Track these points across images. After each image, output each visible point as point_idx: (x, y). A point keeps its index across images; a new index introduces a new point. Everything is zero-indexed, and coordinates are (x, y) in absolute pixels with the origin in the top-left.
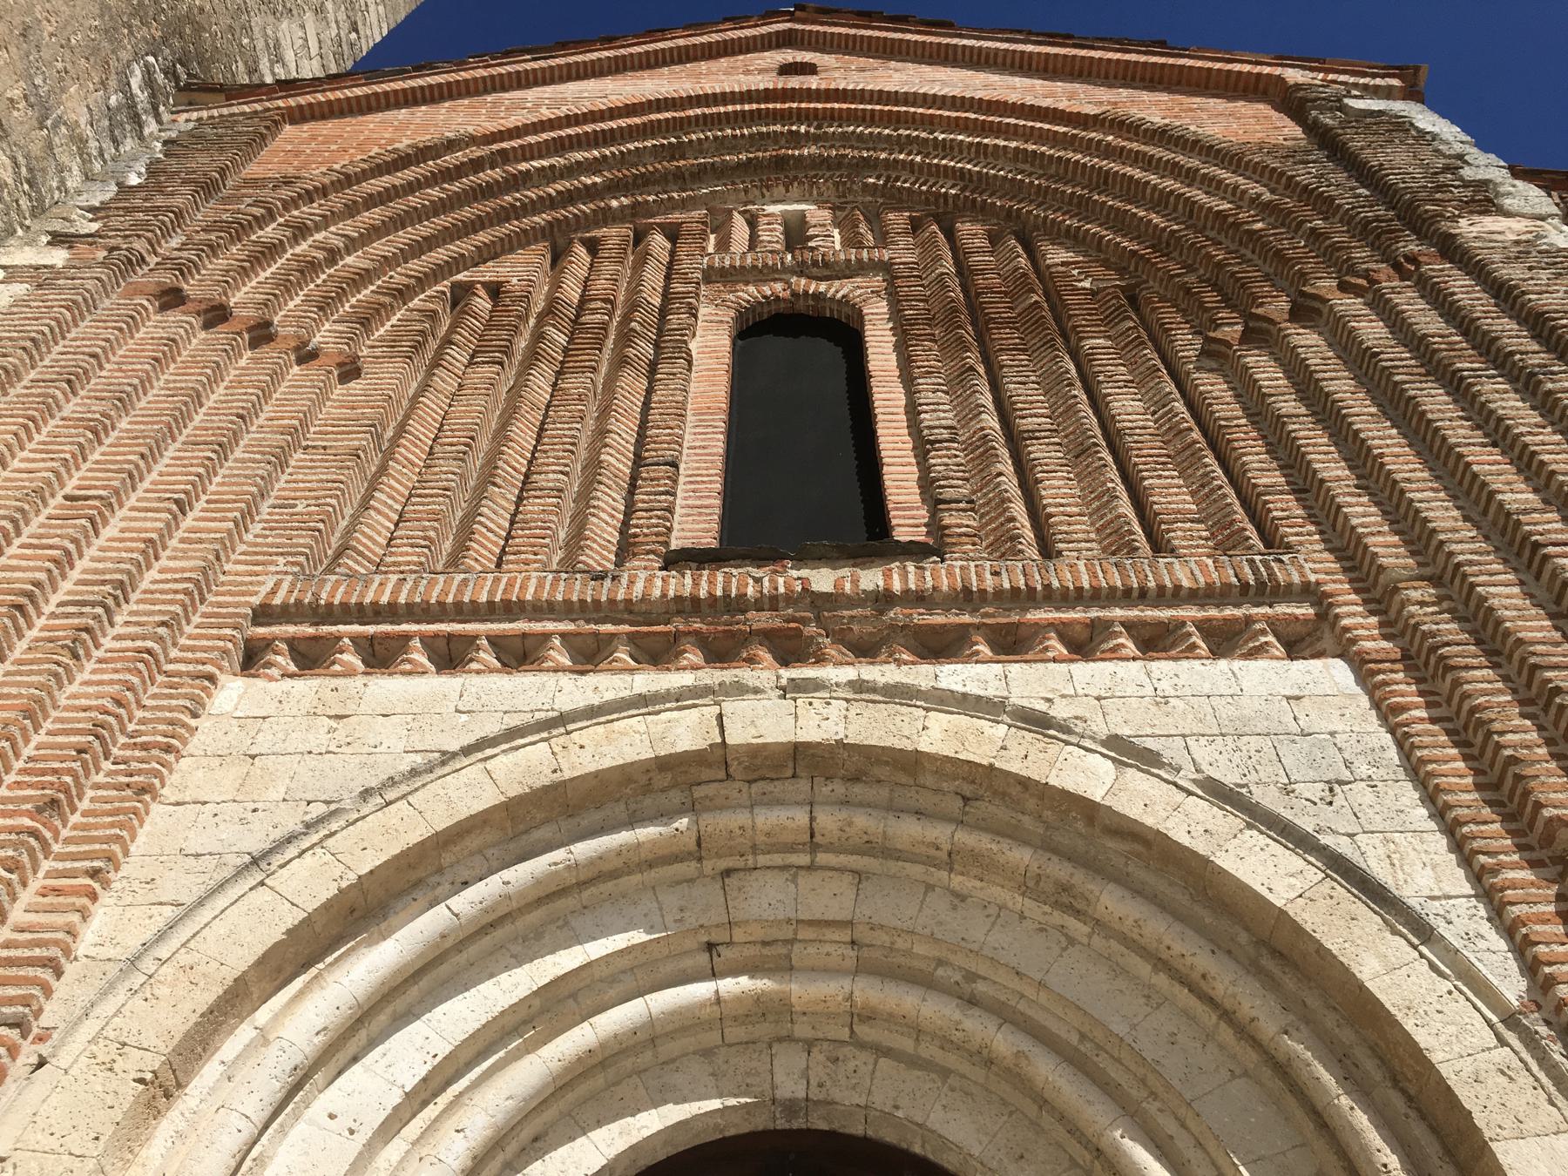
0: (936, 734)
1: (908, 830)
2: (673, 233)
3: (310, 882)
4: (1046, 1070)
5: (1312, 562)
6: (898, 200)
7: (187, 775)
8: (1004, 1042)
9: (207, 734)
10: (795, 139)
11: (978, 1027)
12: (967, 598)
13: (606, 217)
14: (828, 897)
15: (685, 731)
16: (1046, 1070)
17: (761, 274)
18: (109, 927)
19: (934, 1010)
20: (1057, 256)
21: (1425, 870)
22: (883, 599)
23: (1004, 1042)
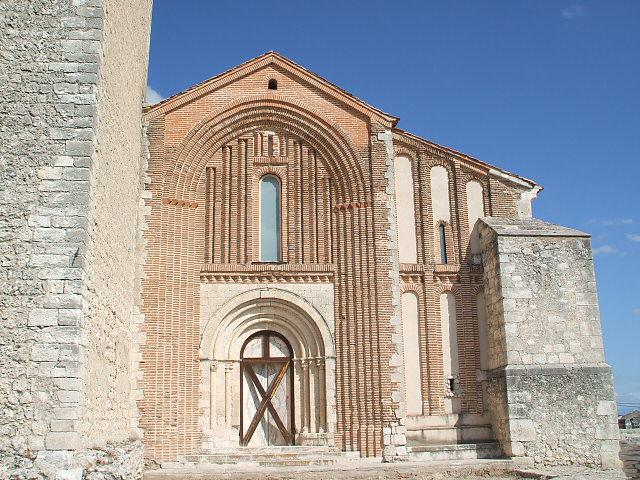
0: (285, 297)
1: (281, 306)
2: (246, 141)
3: (220, 316)
4: (292, 330)
5: (334, 268)
6: (293, 136)
7: (202, 301)
8: (289, 327)
9: (202, 294)
10: (271, 115)
11: (286, 325)
12: (291, 272)
13: (233, 139)
14: (272, 311)
15: (256, 295)
16: (292, 330)
17: (264, 164)
18: (202, 322)
19: (283, 323)
20: (320, 164)
21: (330, 317)
22: (280, 271)
23: (289, 327)
